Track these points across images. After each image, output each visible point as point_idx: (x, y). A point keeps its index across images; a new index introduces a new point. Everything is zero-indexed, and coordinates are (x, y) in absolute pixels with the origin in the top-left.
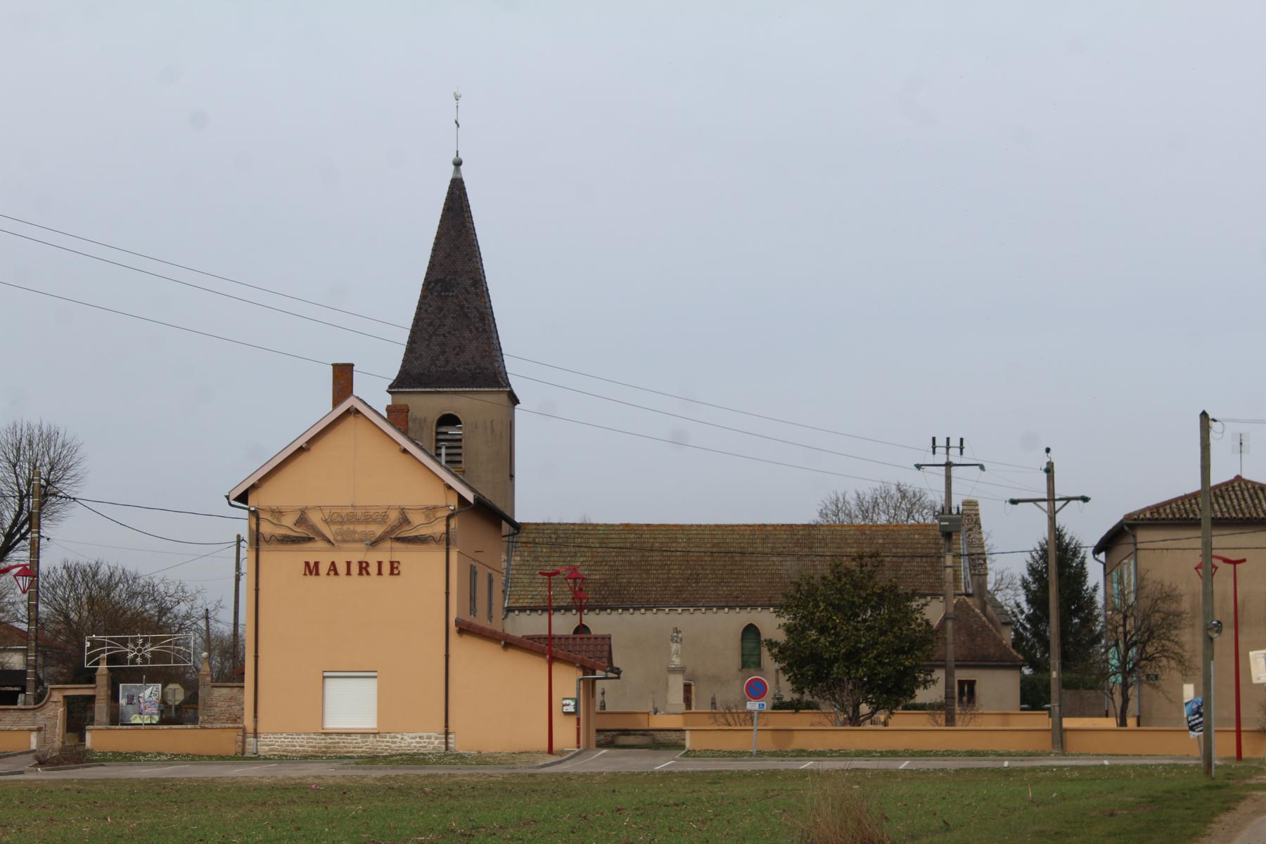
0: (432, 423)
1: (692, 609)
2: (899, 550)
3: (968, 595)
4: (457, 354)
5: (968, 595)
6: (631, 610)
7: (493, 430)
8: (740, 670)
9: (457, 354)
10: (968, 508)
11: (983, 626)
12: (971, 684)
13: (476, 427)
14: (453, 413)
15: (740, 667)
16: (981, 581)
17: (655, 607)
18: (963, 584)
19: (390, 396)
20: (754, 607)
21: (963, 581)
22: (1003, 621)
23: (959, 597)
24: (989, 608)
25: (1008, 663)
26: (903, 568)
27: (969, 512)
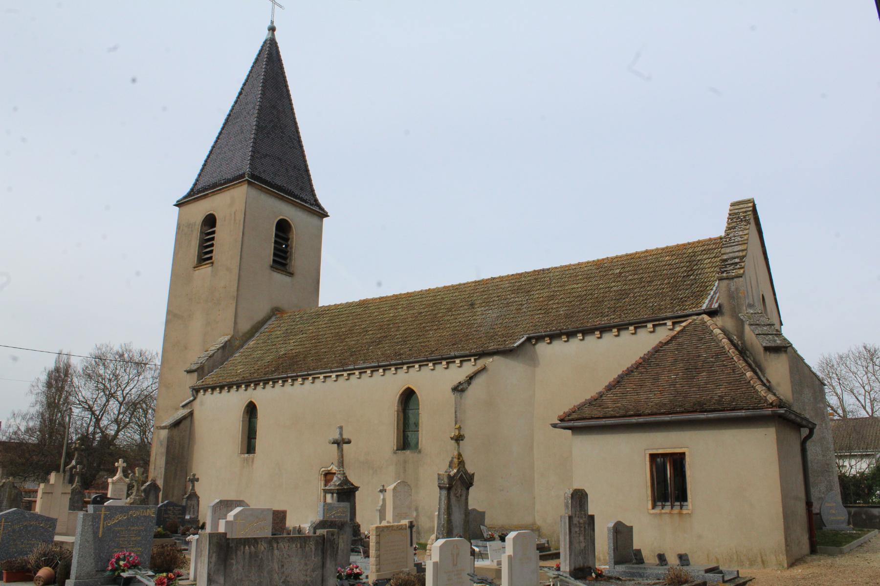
0: (199, 225)
1: (345, 374)
2: (636, 276)
3: (712, 313)
4: (228, 164)
5: (712, 313)
6: (290, 381)
7: (235, 220)
8: (395, 453)
9: (228, 164)
10: (737, 207)
11: (722, 352)
12: (678, 460)
13: (225, 220)
14: (211, 212)
15: (395, 449)
16: (733, 288)
17: (310, 375)
18: (707, 301)
19: (177, 208)
20: (410, 365)
21: (709, 297)
22: (764, 345)
23: (695, 317)
24: (747, 328)
25: (742, 413)
26: (631, 295)
27: (737, 211)
